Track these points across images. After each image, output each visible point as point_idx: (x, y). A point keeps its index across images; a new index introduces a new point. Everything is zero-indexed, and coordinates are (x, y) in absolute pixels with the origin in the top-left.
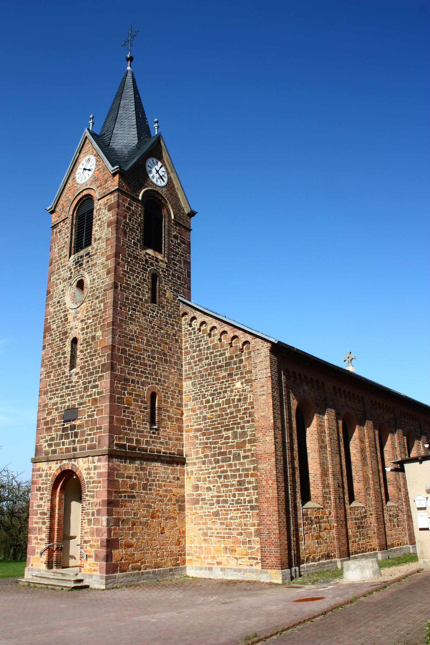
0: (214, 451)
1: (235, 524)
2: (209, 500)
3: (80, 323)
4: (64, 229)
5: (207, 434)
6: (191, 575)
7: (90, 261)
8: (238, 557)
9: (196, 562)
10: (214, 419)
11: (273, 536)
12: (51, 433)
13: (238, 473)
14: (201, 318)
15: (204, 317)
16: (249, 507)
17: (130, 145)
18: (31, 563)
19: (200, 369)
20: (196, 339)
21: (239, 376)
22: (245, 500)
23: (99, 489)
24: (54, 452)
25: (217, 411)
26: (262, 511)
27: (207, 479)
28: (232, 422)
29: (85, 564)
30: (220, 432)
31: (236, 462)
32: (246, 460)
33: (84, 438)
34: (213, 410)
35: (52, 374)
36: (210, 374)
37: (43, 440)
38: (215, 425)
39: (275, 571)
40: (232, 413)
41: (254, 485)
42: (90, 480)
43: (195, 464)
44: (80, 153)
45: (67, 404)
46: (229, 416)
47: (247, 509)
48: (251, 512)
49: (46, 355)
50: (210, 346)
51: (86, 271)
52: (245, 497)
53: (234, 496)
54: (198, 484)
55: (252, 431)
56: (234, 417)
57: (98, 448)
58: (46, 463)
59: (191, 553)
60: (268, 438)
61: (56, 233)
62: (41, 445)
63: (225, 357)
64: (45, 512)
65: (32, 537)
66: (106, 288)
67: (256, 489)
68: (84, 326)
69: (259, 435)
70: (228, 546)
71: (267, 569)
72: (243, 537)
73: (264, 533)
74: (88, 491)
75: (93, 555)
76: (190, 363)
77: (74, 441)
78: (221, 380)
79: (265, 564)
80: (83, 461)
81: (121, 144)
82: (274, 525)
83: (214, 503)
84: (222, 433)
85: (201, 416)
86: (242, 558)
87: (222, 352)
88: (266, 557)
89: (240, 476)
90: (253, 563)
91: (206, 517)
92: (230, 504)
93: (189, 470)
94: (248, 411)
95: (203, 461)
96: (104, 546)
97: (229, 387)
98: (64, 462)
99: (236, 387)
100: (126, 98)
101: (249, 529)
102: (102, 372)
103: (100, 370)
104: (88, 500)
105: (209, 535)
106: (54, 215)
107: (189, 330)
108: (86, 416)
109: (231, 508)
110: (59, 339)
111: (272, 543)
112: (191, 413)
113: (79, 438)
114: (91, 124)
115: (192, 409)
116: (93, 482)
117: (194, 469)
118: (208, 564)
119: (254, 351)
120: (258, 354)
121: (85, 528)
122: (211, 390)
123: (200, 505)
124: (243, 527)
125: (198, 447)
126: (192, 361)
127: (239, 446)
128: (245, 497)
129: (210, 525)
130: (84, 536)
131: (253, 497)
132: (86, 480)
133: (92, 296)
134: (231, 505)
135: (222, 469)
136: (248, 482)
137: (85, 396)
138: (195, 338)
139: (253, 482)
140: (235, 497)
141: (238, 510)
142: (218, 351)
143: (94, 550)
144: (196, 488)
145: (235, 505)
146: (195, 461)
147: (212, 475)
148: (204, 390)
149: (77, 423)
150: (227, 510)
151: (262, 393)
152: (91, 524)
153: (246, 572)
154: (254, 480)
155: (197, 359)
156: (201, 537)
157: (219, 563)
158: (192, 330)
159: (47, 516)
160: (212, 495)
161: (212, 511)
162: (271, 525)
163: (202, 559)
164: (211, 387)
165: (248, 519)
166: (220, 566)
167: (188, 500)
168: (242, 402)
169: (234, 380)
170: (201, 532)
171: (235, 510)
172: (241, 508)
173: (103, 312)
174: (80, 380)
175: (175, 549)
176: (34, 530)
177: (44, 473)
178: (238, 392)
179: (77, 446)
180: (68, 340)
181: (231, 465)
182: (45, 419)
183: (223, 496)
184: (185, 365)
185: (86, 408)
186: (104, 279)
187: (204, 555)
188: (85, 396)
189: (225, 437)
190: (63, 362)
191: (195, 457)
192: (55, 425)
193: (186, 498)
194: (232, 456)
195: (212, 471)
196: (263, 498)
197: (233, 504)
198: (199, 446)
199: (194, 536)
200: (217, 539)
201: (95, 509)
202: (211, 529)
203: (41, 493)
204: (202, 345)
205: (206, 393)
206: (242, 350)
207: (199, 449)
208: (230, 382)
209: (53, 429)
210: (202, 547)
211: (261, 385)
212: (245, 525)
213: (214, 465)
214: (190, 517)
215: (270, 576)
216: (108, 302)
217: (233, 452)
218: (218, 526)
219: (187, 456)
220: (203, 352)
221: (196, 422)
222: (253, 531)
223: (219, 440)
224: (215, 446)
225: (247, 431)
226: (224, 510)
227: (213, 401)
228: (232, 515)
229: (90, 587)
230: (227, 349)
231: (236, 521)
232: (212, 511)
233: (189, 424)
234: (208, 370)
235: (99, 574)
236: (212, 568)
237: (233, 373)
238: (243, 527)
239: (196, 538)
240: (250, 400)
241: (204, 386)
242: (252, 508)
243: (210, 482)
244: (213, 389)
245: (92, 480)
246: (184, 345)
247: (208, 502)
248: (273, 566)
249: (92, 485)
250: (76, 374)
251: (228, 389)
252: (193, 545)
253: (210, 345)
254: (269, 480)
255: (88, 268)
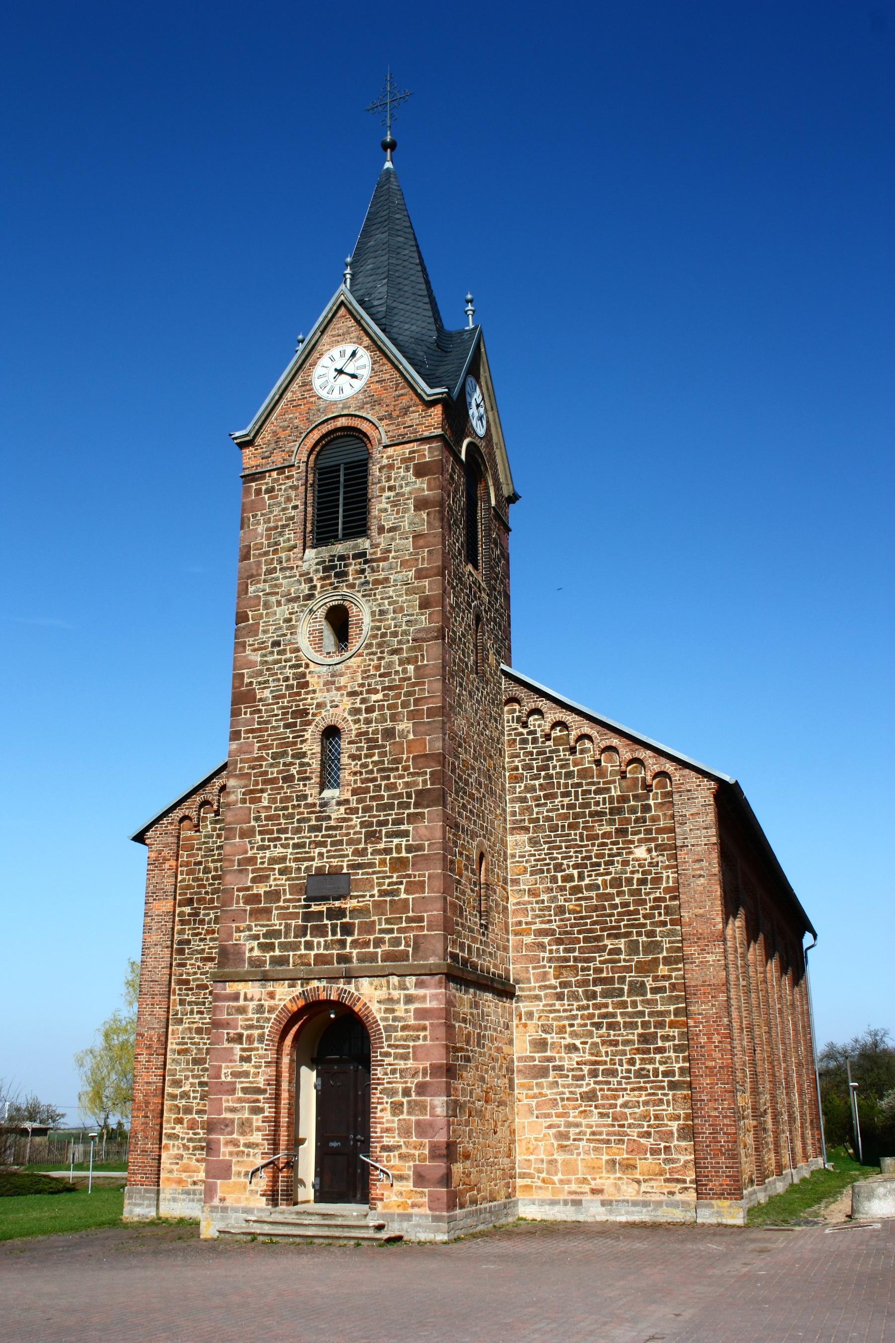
0: (583, 975)
1: (633, 1116)
2: (573, 1070)
3: (345, 699)
4: (283, 487)
5: (566, 941)
6: (529, 1217)
7: (368, 570)
8: (641, 1178)
9: (540, 1191)
10: (584, 914)
11: (722, 1138)
12: (270, 920)
13: (639, 1020)
14: (553, 714)
15: (562, 712)
16: (665, 1084)
17: (425, 338)
18: (219, 1194)
19: (550, 814)
20: (538, 754)
21: (642, 836)
22: (656, 1071)
23: (421, 1042)
24: (275, 961)
25: (591, 898)
26: (699, 1092)
27: (568, 1029)
28: (626, 922)
29: (386, 1193)
30: (599, 939)
31: (635, 998)
32: (658, 996)
33: (372, 937)
34: (580, 895)
35: (265, 795)
36: (572, 826)
37: (242, 934)
38: (586, 924)
39: (727, 1203)
40: (625, 905)
41: (677, 1042)
42: (396, 1024)
43: (538, 998)
44: (323, 332)
45: (316, 864)
46: (619, 910)
47: (663, 1088)
48: (671, 1093)
49: (240, 751)
50: (573, 771)
51: (359, 591)
52: (657, 1065)
53: (632, 1062)
54: (546, 1039)
55: (673, 942)
56: (629, 913)
57: (414, 960)
58: (257, 984)
59: (529, 1174)
60: (710, 958)
61: (258, 492)
62: (236, 944)
63: (610, 797)
64: (259, 1088)
65: (219, 1140)
66: (419, 635)
67: (682, 1051)
68: (358, 705)
69: (691, 950)
70: (618, 1158)
71: (711, 1199)
72: (651, 1140)
73: (704, 1133)
74: (389, 1046)
75: (408, 1175)
76: (523, 800)
77: (343, 943)
78: (600, 841)
79: (706, 1189)
80: (371, 984)
81: (408, 333)
82: (725, 1117)
83: (584, 1075)
84: (603, 941)
85: (553, 905)
86: (651, 1179)
87: (601, 786)
88: (707, 1176)
89: (645, 1025)
90: (676, 1190)
91: (566, 1102)
92: (622, 1078)
93: (523, 1010)
94: (663, 904)
95: (557, 993)
96: (440, 1156)
97: (619, 854)
98: (315, 984)
99: (636, 856)
100: (399, 233)
101: (667, 1125)
102: (416, 805)
103: (413, 801)
104: (390, 1065)
105: (572, 1137)
106: (247, 451)
107: (522, 734)
108: (375, 892)
109: (624, 1086)
110: (282, 723)
111: (720, 1150)
112: (526, 898)
113: (356, 937)
114: (348, 276)
115: (529, 890)
116: (404, 1028)
117: (534, 1009)
118: (570, 1193)
119: (679, 792)
120: (688, 799)
121: (384, 1120)
122: (577, 857)
123: (551, 1079)
124: (652, 1122)
125: (544, 966)
126: (528, 795)
127: (643, 968)
128: (657, 1065)
129: (574, 1117)
130: (382, 1137)
131: (674, 1065)
132: (382, 1024)
133: (380, 645)
134: (624, 1081)
135: (604, 1010)
136: (662, 1036)
137: (370, 850)
138: (535, 751)
139: (674, 1036)
140: (633, 1064)
141: (641, 1089)
142: (593, 783)
143: (411, 1164)
144: (541, 1045)
145: (633, 1080)
146: (537, 992)
147: (579, 1021)
148: (559, 856)
149: (350, 904)
150: (616, 1090)
151: (698, 872)
152: (402, 1113)
153: (661, 1207)
154: (676, 1034)
155: (542, 794)
156: (553, 1141)
157: (594, 1191)
158: (529, 733)
159: (267, 1096)
160: (580, 1059)
161: (578, 1090)
162: (718, 1117)
163: (554, 1183)
164: (576, 852)
165: (665, 1107)
166: (600, 1197)
167: (520, 1068)
168: (649, 886)
169: (632, 842)
170: (554, 1130)
171: (633, 1090)
172: (648, 1085)
173: (414, 685)
174: (354, 816)
175: (504, 1162)
176: (227, 1126)
177: (252, 1005)
178: (640, 866)
179: (351, 953)
180: (311, 728)
181: (623, 1005)
182: (248, 889)
183: (605, 1063)
184: (512, 801)
185: (375, 876)
186: (412, 615)
187: (560, 1176)
188: (370, 850)
189: (610, 949)
190: (299, 773)
191: (537, 985)
192: (281, 904)
193: (516, 1064)
194: (626, 988)
195: (579, 1013)
196: (701, 1068)
197: (630, 1078)
198: (548, 965)
199: (536, 1139)
200: (592, 1145)
201: (412, 1083)
202: (577, 1125)
203: (245, 1046)
204: (554, 767)
205: (565, 862)
206: (648, 788)
207: (547, 969)
208: (621, 846)
209: (275, 912)
210: (556, 1161)
211: (696, 857)
212: (657, 1117)
213: (585, 1002)
214: (525, 1101)
215: (718, 1212)
216: (426, 665)
217: (628, 979)
218: (595, 1119)
219: (517, 981)
220: (555, 781)
221: (540, 917)
222: (675, 1129)
223: (597, 955)
224: (585, 965)
225: (662, 941)
226: (609, 1089)
227: (581, 877)
228: (626, 1098)
229: (405, 1238)
230: (614, 782)
231: (636, 1110)
232: (578, 1090)
233: (524, 920)
234: (568, 818)
235: (429, 1212)
236: (581, 1201)
237: (627, 828)
238: (652, 1122)
239: (540, 1143)
240: (668, 882)
241: (560, 847)
242: (673, 1086)
243: (574, 1034)
244: (580, 856)
245: (401, 1024)
246: (508, 762)
247: (570, 1074)
248: (723, 1194)
249: (400, 1034)
250: (339, 803)
251: (616, 859)
252: (532, 1157)
253: (572, 768)
254: (713, 1034)
255: (362, 584)
